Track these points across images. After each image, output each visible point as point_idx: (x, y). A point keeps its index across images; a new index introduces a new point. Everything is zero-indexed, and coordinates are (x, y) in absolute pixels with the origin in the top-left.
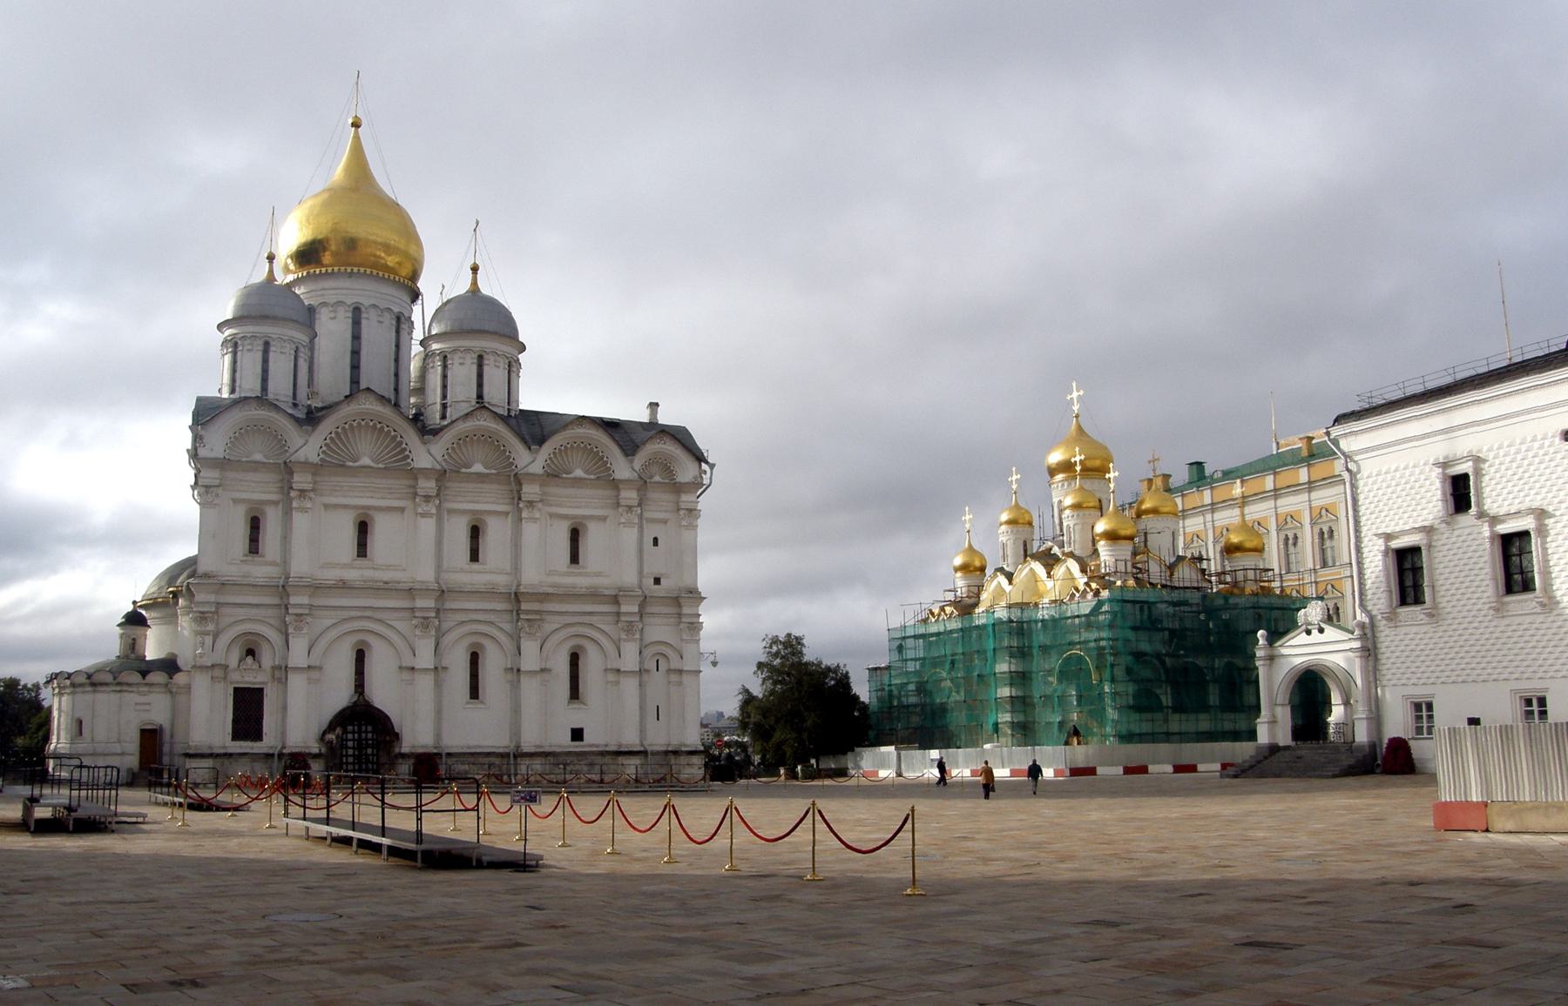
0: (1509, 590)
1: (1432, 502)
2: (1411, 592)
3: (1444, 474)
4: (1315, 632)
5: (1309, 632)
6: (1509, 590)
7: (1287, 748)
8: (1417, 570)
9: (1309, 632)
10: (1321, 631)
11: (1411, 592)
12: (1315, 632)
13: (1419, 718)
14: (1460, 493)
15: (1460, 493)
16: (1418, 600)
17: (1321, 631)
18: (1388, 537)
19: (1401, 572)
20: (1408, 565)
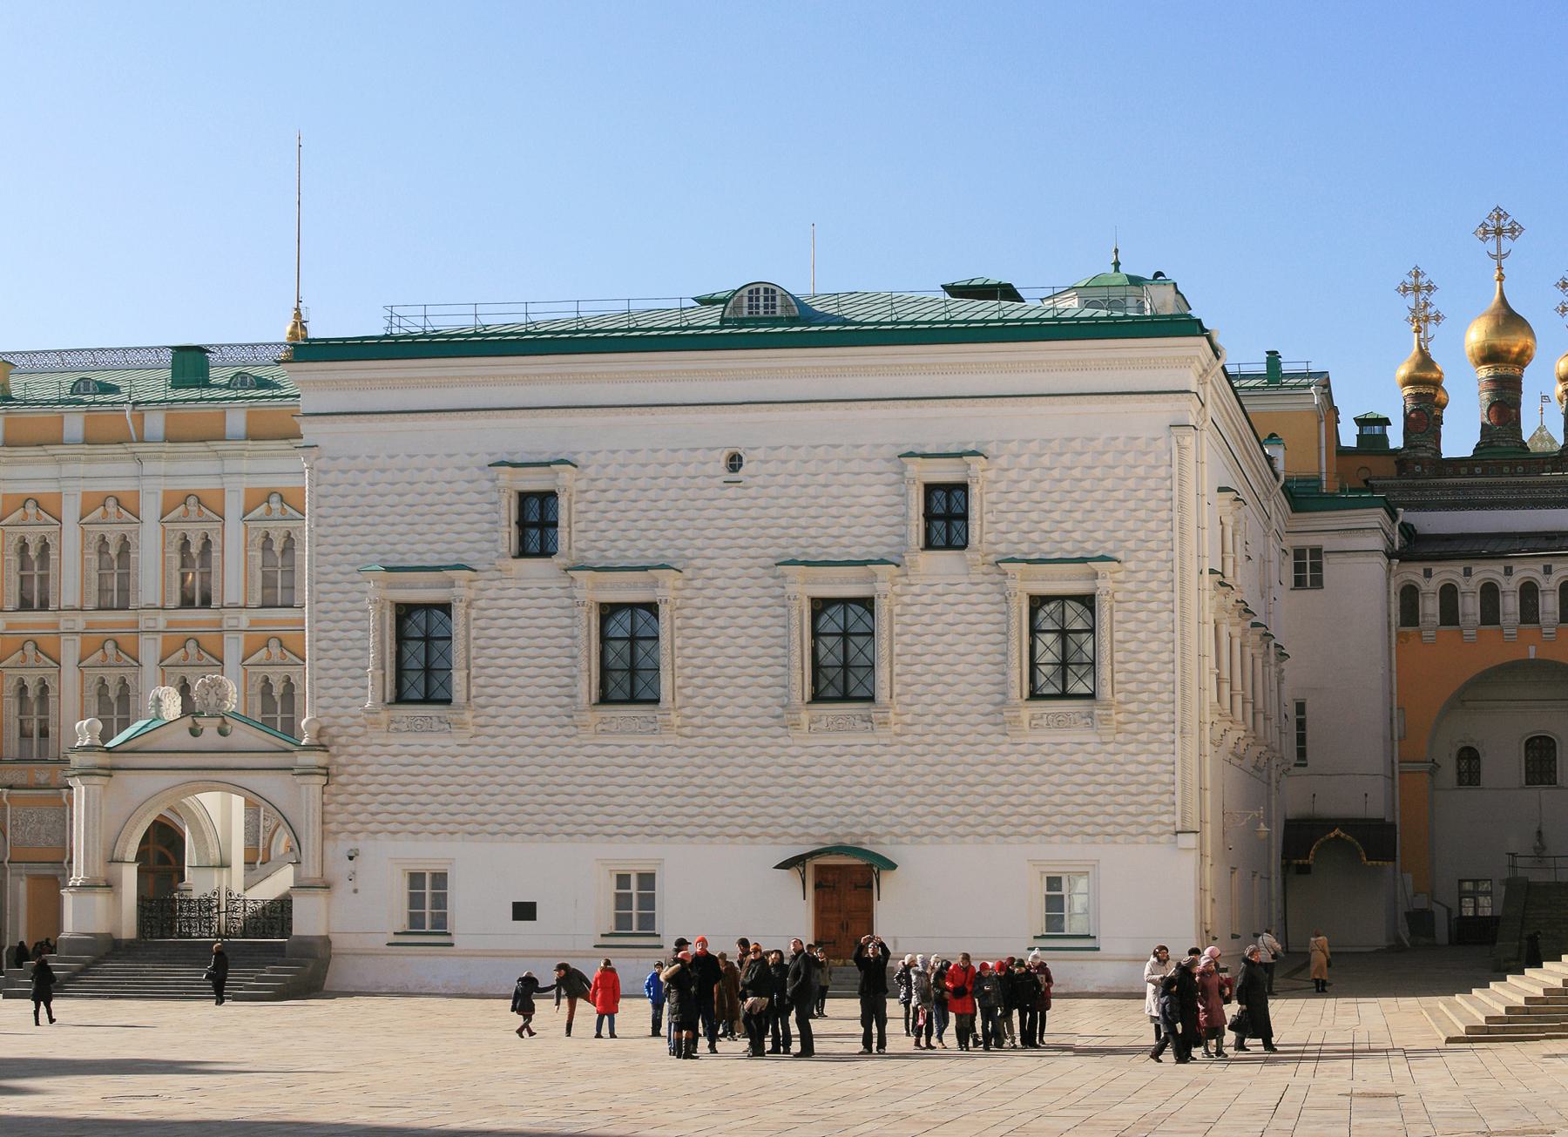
15: (536, 523)
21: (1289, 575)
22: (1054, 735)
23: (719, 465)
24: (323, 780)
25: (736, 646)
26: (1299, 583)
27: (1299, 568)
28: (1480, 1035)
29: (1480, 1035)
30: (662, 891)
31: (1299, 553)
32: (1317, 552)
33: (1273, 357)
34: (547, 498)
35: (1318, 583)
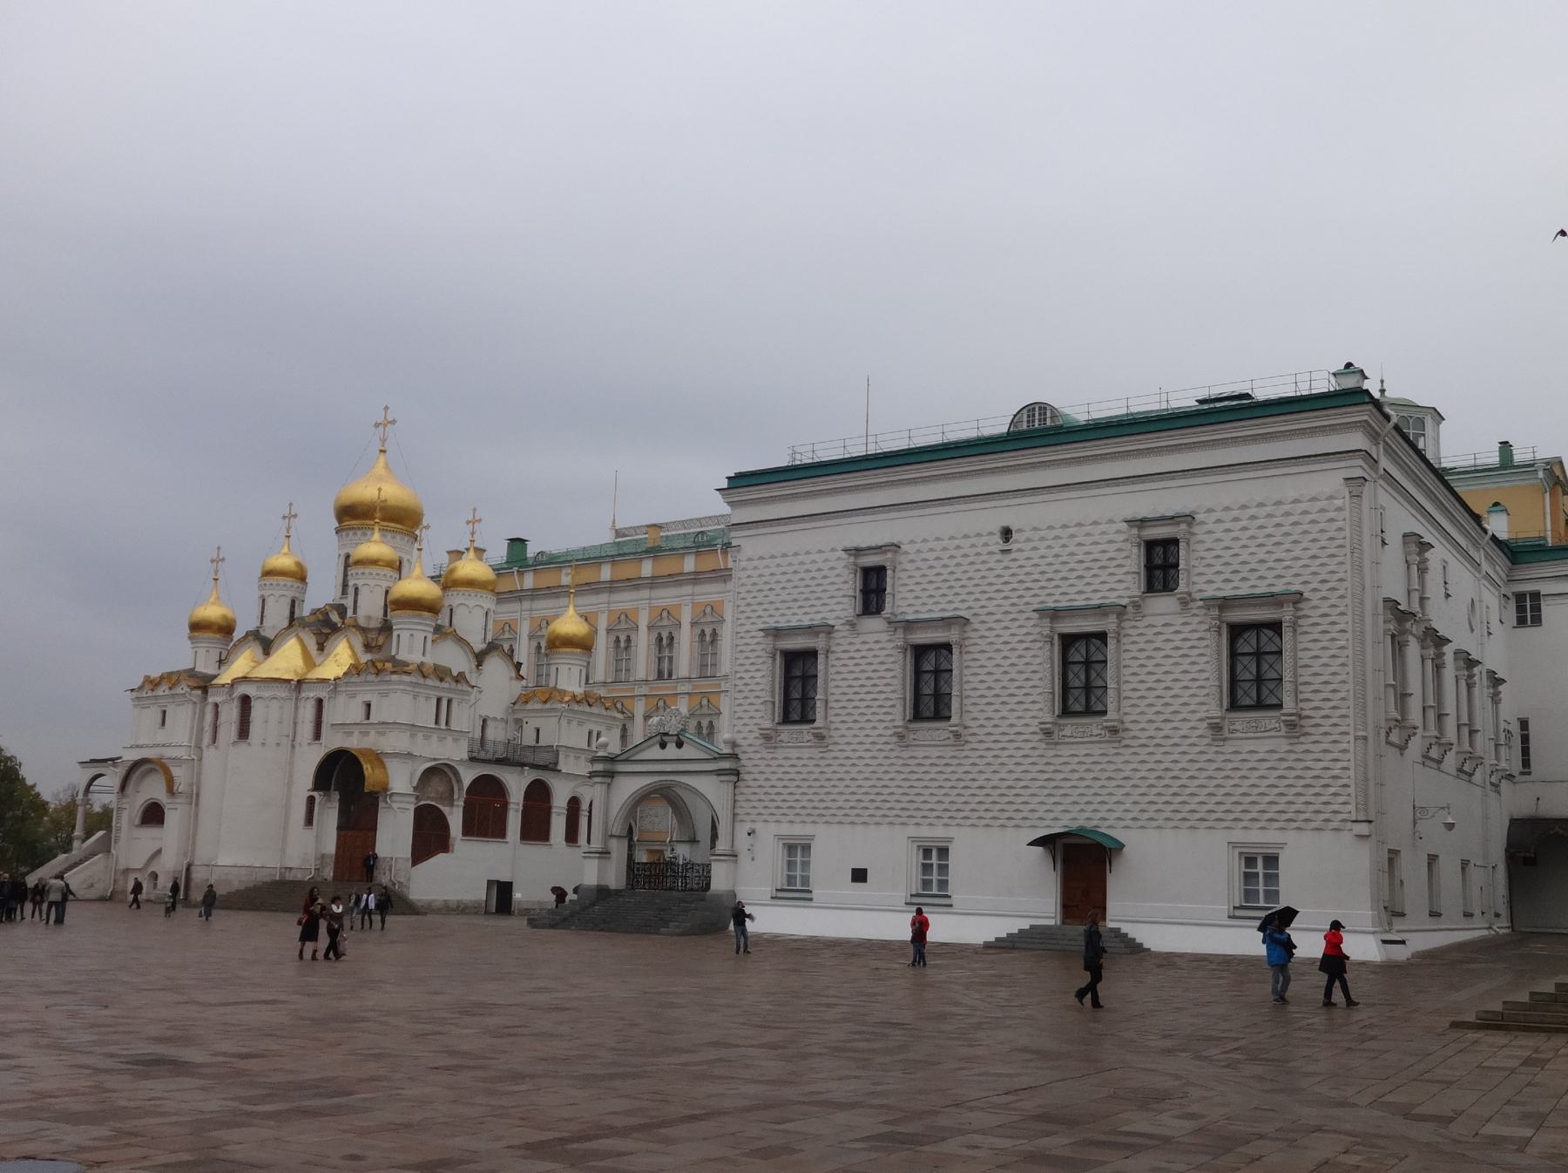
0: (917, 716)
1: (836, 599)
2: (796, 705)
3: (855, 564)
4: (671, 747)
5: (663, 745)
6: (917, 716)
7: (617, 892)
8: (809, 679)
9: (663, 745)
10: (680, 745)
11: (796, 705)
12: (671, 747)
13: (791, 865)
14: (873, 587)
15: (873, 587)
16: (806, 719)
17: (680, 745)
18: (776, 633)
19: (788, 679)
20: (797, 672)
21: (1511, 613)
22: (1258, 740)
23: (996, 542)
24: (734, 778)
25: (1006, 677)
26: (1521, 622)
27: (1521, 609)
28: (1489, 1023)
29: (1489, 1023)
30: (953, 860)
31: (1520, 597)
32: (1536, 596)
33: (1505, 445)
34: (880, 571)
35: (1537, 620)
